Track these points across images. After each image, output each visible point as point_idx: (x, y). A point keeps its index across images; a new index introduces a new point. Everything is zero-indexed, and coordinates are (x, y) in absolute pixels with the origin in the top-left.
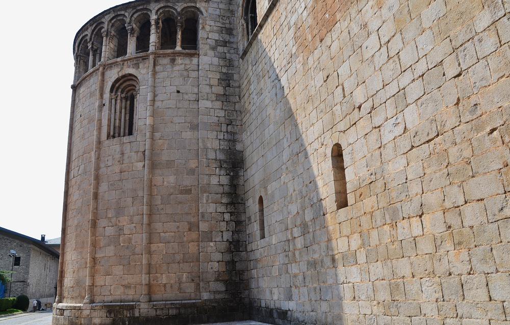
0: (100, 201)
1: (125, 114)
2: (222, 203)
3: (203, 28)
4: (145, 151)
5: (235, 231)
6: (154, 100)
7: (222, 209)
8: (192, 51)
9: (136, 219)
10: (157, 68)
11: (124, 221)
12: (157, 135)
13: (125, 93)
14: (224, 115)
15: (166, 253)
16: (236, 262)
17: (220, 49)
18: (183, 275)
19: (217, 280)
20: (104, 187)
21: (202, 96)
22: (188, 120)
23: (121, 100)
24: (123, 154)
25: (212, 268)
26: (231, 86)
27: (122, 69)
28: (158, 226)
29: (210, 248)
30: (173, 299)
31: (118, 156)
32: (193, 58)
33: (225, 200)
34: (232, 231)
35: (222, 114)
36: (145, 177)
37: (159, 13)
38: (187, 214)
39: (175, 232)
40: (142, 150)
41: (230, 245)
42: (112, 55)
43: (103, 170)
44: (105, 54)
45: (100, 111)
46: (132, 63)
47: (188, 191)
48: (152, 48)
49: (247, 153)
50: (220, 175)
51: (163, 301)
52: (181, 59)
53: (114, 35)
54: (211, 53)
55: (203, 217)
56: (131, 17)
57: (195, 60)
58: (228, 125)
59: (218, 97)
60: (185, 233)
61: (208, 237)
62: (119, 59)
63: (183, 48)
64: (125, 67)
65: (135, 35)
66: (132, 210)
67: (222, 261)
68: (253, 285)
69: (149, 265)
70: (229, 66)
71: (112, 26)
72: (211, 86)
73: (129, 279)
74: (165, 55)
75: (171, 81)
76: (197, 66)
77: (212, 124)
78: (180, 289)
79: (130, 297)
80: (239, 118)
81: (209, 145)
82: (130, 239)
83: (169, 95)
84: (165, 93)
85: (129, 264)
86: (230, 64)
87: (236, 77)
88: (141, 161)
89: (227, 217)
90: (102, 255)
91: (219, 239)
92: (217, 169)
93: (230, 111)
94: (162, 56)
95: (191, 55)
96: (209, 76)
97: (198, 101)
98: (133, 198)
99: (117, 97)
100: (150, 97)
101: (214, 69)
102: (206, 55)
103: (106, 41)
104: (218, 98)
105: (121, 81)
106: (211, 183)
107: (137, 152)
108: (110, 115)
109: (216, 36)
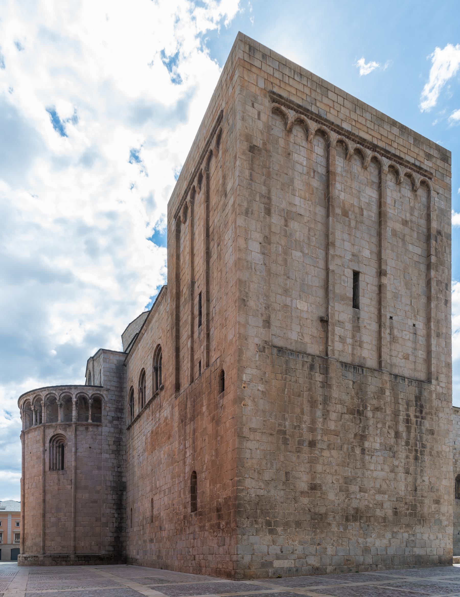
1: (59, 456)
6: (76, 452)
7: (113, 511)
10: (78, 432)
12: (79, 471)
13: (58, 443)
19: (109, 545)
23: (56, 448)
24: (59, 480)
27: (56, 430)
33: (115, 507)
40: (70, 479)
47: (96, 502)
49: (128, 484)
54: (109, 425)
55: (103, 515)
57: (100, 429)
59: (113, 452)
61: (106, 525)
62: (54, 424)
63: (92, 419)
68: (127, 548)
69: (75, 537)
72: (109, 445)
80: (125, 464)
81: (107, 479)
86: (121, 432)
87: (124, 440)
89: (116, 515)
91: (111, 526)
95: (98, 426)
100: (73, 450)
102: (106, 426)
103: (44, 409)
108: (50, 456)
109: (113, 414)
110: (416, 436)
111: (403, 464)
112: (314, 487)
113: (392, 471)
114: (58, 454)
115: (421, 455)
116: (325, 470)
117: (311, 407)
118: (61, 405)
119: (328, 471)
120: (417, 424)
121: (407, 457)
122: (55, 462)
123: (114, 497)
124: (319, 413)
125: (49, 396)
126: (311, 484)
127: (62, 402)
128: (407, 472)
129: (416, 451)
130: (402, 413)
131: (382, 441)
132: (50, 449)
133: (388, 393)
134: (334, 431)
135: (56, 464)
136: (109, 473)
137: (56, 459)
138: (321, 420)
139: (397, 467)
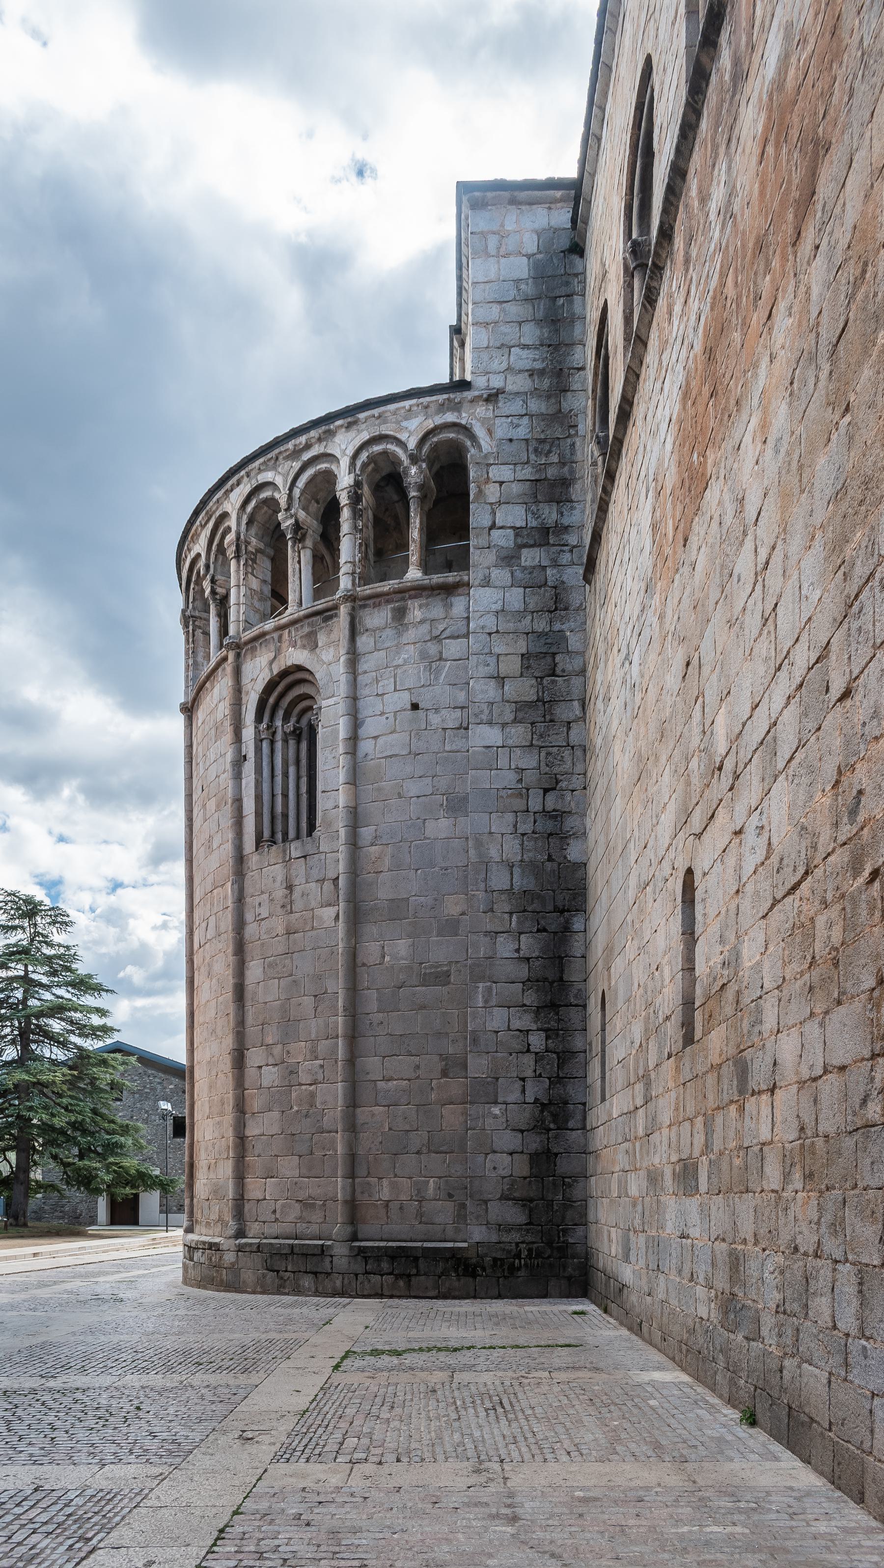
0: (248, 1003)
2: (524, 1005)
3: (480, 492)
4: (337, 878)
5: (558, 1076)
7: (525, 1021)
8: (451, 577)
9: (323, 1046)
10: (364, 642)
11: (299, 1050)
13: (293, 720)
14: (534, 764)
15: (390, 1129)
16: (556, 1155)
17: (530, 557)
18: (428, 1181)
20: (254, 971)
21: (476, 715)
22: (443, 783)
23: (285, 741)
25: (495, 1168)
26: (558, 671)
27: (278, 652)
28: (372, 1064)
29: (491, 1121)
30: (404, 1237)
31: (280, 893)
32: (453, 599)
33: (530, 998)
34: (549, 1078)
35: (529, 761)
36: (340, 946)
37: (359, 464)
38: (439, 1034)
39: (409, 1080)
41: (542, 1111)
42: (257, 611)
43: (251, 930)
44: (238, 612)
45: (238, 776)
46: (300, 633)
48: (345, 583)
50: (520, 933)
51: (382, 1240)
52: (420, 607)
53: (258, 551)
56: (291, 489)
58: (546, 791)
60: (434, 1082)
62: (269, 625)
64: (285, 645)
65: (309, 543)
66: (314, 1027)
67: (522, 1152)
70: (556, 609)
71: (250, 523)
73: (312, 1188)
74: (378, 599)
75: (395, 676)
76: (464, 622)
77: (503, 793)
78: (420, 1214)
79: (314, 1229)
81: (494, 853)
82: (313, 1095)
83: (392, 719)
84: (382, 714)
85: (312, 1153)
88: (330, 905)
89: (537, 1041)
90: (257, 1132)
92: (514, 916)
93: (555, 750)
94: (370, 602)
96: (497, 650)
97: (467, 729)
98: (315, 996)
99: (274, 733)
101: (511, 626)
103: (238, 571)
104: (520, 715)
105: (279, 689)
106: (498, 956)
107: (322, 881)
114: (292, 770)
118: (297, 526)
122: (279, 809)
123: (528, 944)
125: (253, 504)
127: (302, 514)
132: (258, 750)
135: (285, 816)
136: (502, 824)
137: (285, 796)
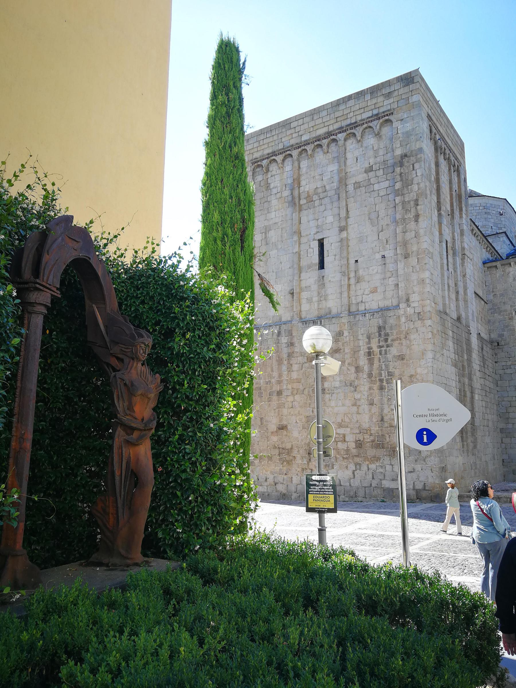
110: (380, 366)
111: (366, 396)
112: (282, 428)
113: (354, 405)
115: (387, 383)
116: (290, 413)
117: (279, 365)
119: (292, 413)
120: (380, 354)
121: (370, 388)
124: (284, 368)
126: (279, 425)
128: (371, 404)
129: (381, 381)
130: (362, 347)
131: (342, 378)
133: (346, 333)
134: (297, 379)
138: (286, 373)
139: (359, 400)
